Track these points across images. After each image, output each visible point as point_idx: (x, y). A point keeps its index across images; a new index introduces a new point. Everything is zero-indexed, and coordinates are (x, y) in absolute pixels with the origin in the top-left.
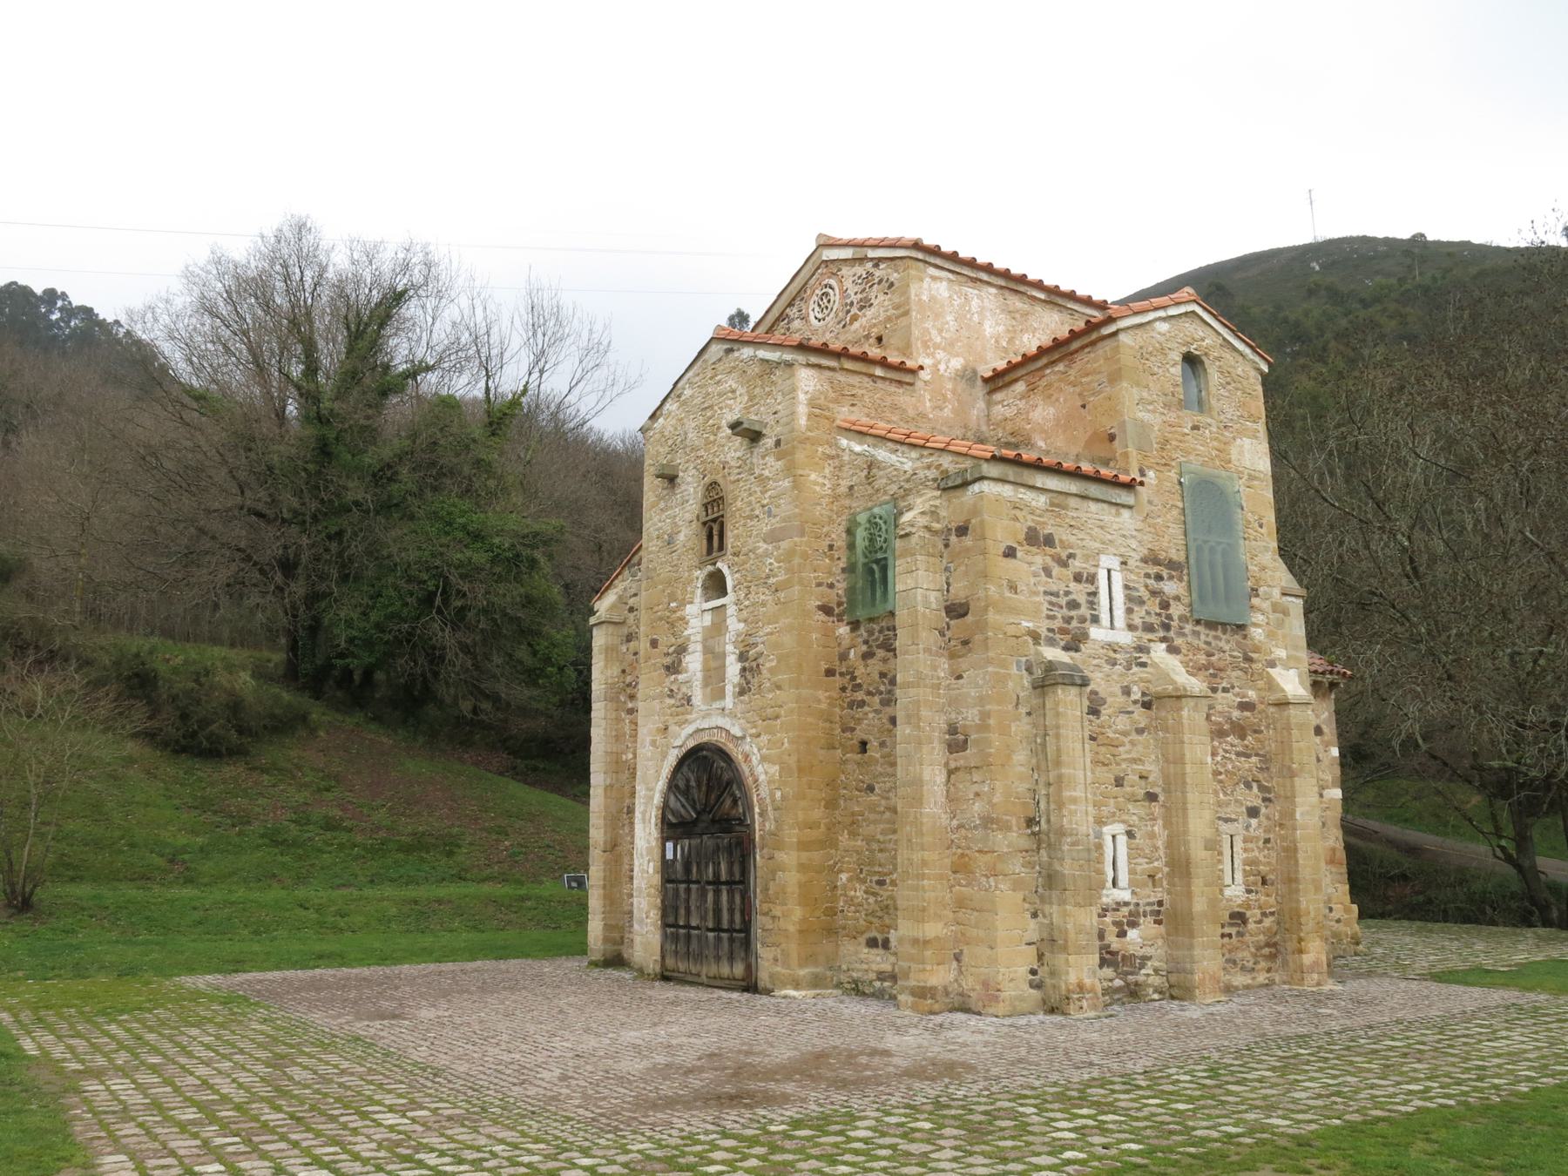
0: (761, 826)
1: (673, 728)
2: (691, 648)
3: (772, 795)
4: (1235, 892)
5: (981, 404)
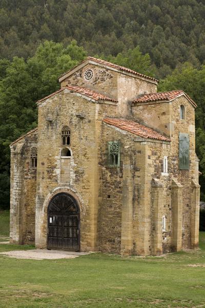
5: (130, 109)
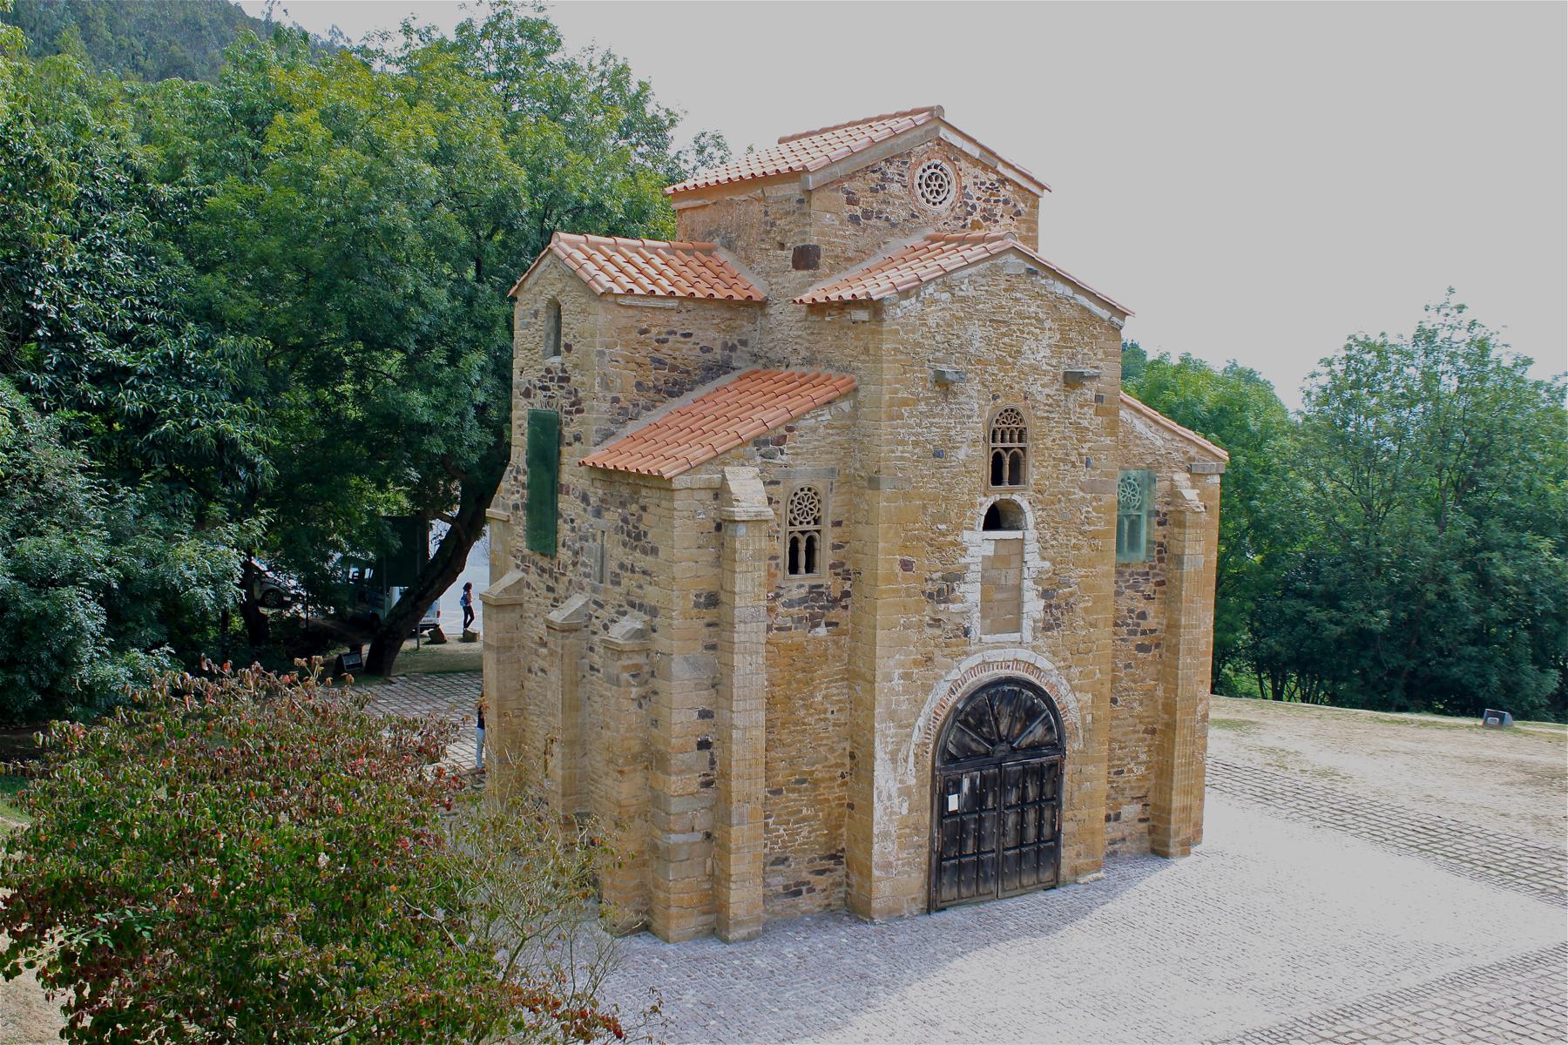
1: (938, 658)
2: (969, 577)
3: (1083, 718)
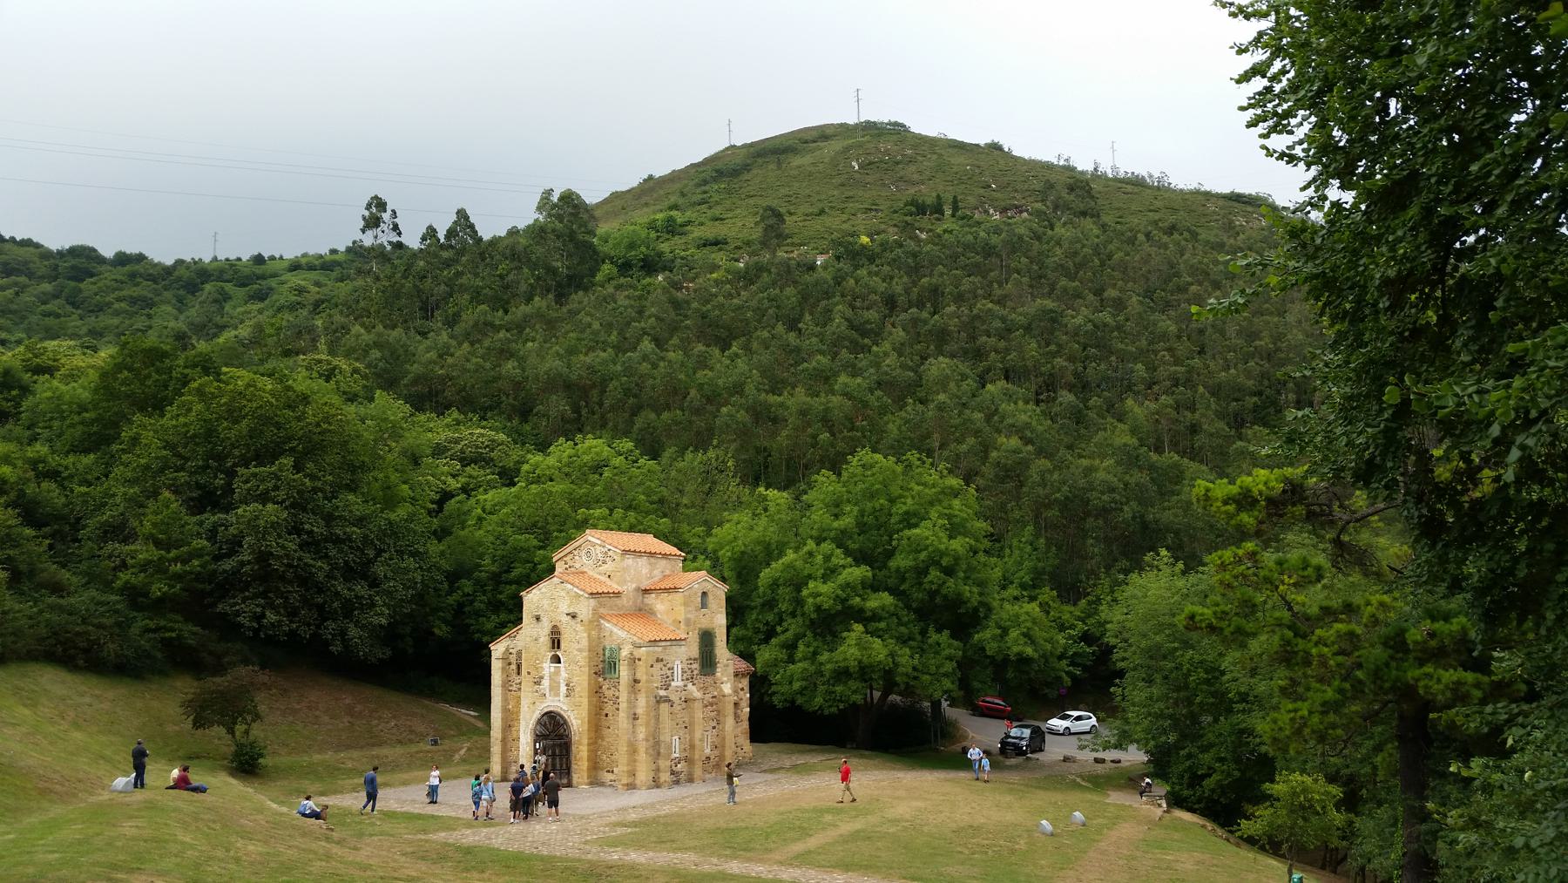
0: (575, 738)
4: (708, 751)
